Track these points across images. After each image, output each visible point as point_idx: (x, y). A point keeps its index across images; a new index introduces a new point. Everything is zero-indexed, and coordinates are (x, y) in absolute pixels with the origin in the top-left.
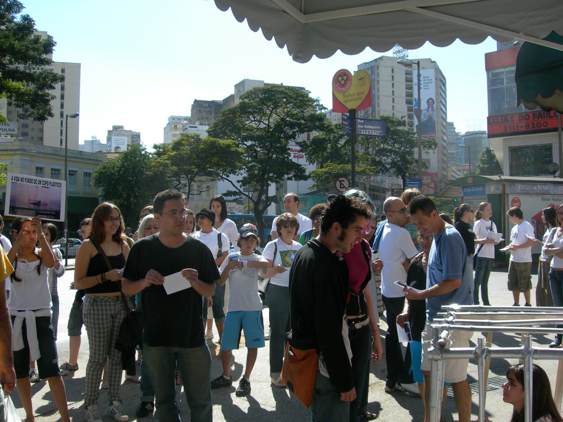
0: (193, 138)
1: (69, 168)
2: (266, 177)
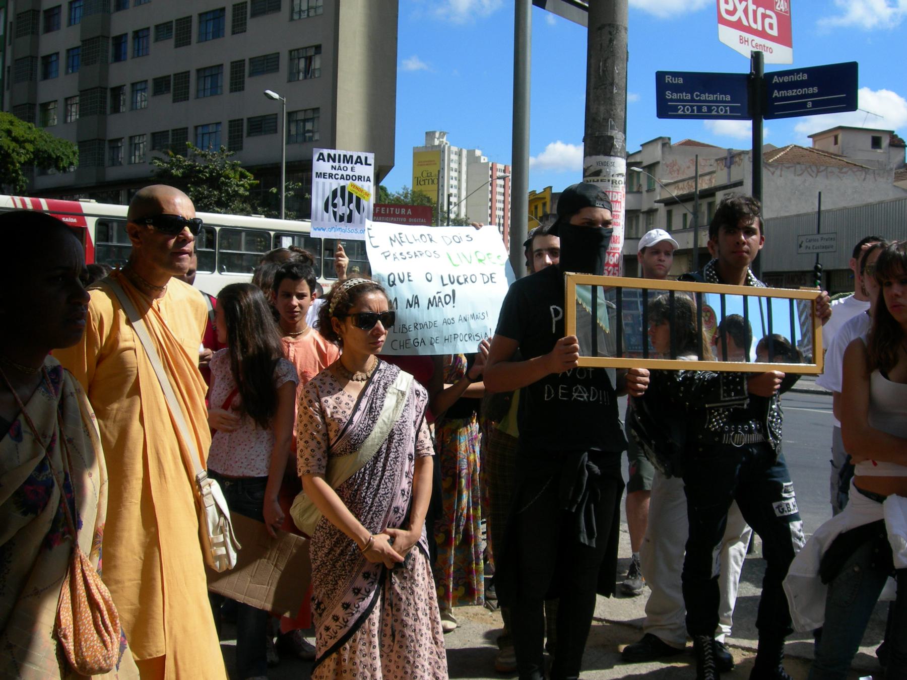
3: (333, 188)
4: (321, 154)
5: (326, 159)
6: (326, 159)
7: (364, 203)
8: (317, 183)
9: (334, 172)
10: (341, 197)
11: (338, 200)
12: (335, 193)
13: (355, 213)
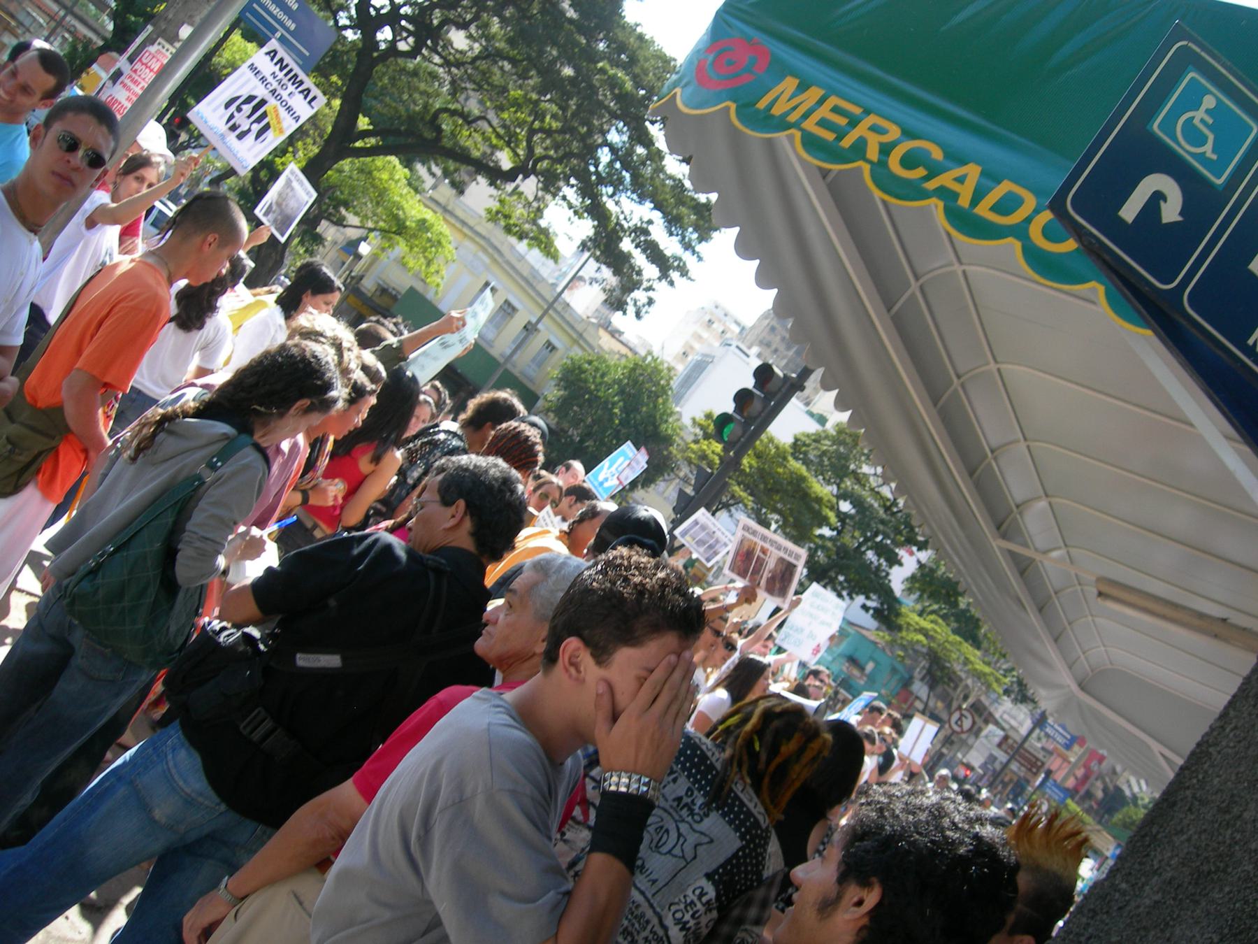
0: (777, 448)
1: (540, 326)
2: (833, 574)
3: (254, 93)
4: (275, 52)
5: (275, 60)
6: (275, 60)
7: (270, 135)
8: (244, 74)
9: (270, 79)
10: (254, 107)
11: (247, 108)
12: (250, 99)
13: (252, 136)
